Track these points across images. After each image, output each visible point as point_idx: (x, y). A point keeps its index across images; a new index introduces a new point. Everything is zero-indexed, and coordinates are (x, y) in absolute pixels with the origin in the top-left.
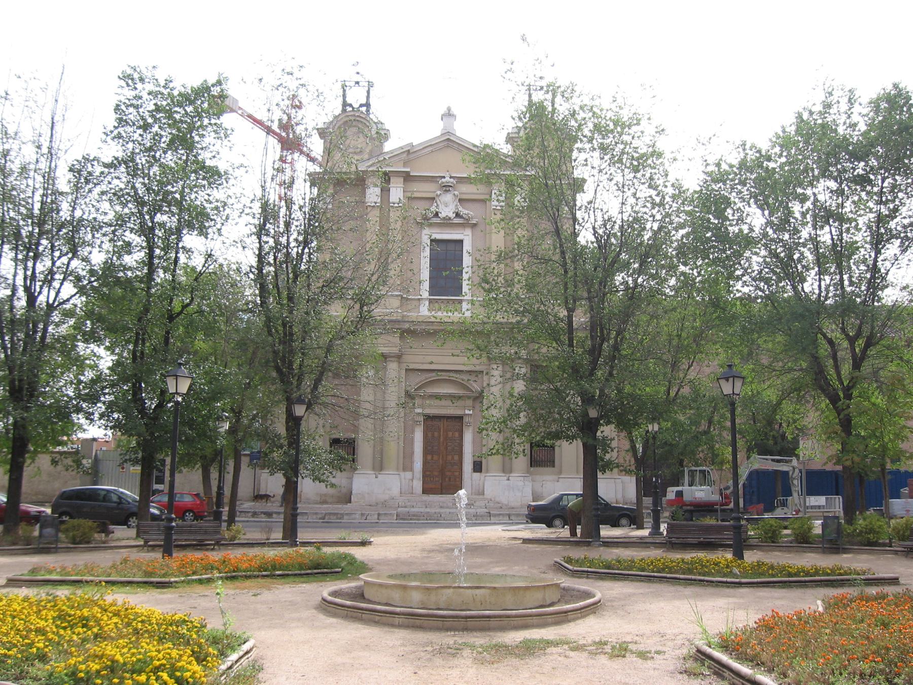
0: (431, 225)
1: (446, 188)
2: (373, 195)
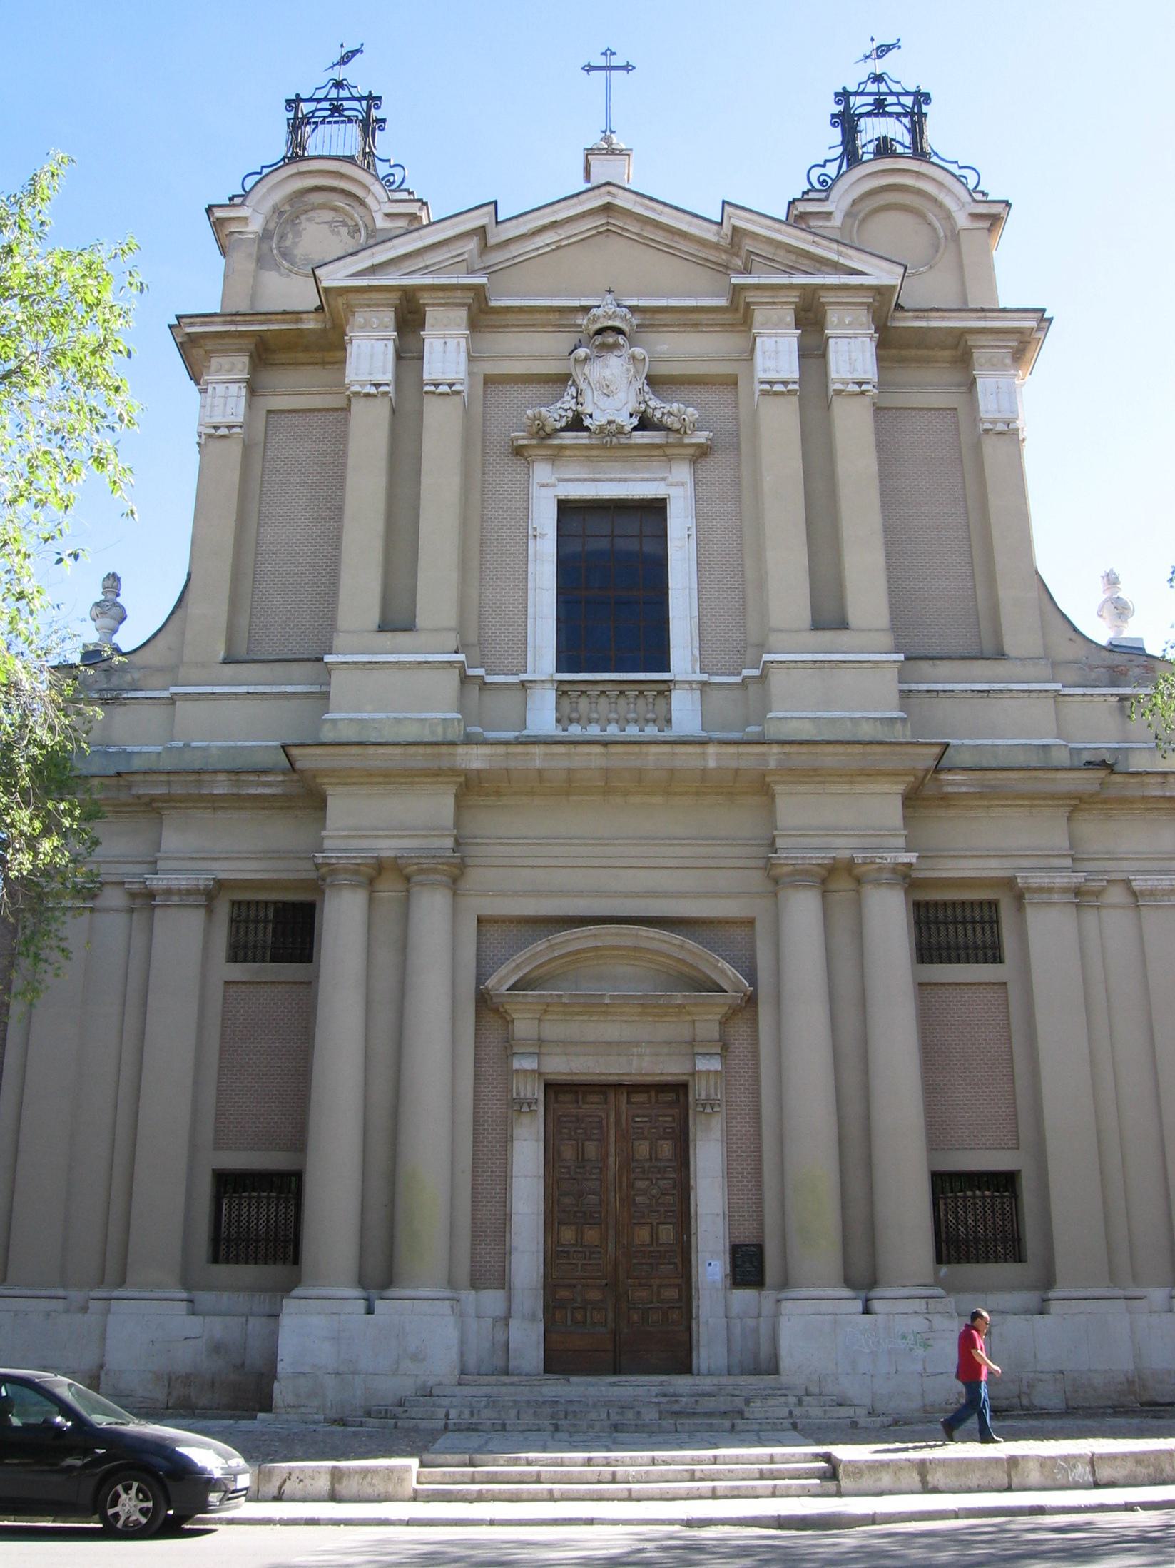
0: (558, 455)
1: (606, 338)
2: (370, 355)
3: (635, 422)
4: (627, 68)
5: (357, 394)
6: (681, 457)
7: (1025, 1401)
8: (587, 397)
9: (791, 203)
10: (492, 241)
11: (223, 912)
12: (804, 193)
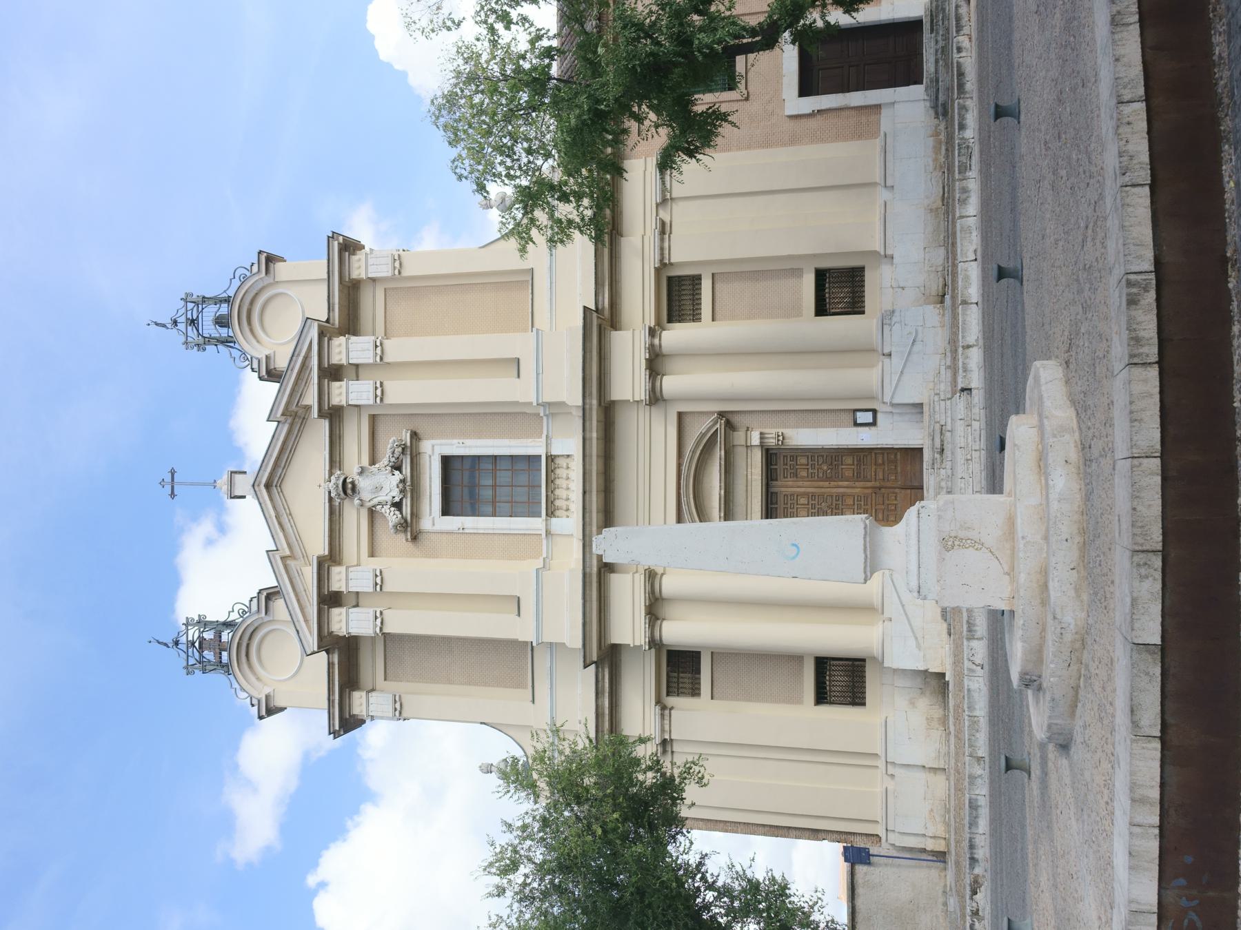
0: (415, 514)
3: (397, 472)
4: (173, 473)
5: (381, 629)
6: (417, 447)
7: (940, 269)
8: (381, 499)
9: (261, 378)
10: (288, 553)
11: (672, 701)
12: (253, 370)
